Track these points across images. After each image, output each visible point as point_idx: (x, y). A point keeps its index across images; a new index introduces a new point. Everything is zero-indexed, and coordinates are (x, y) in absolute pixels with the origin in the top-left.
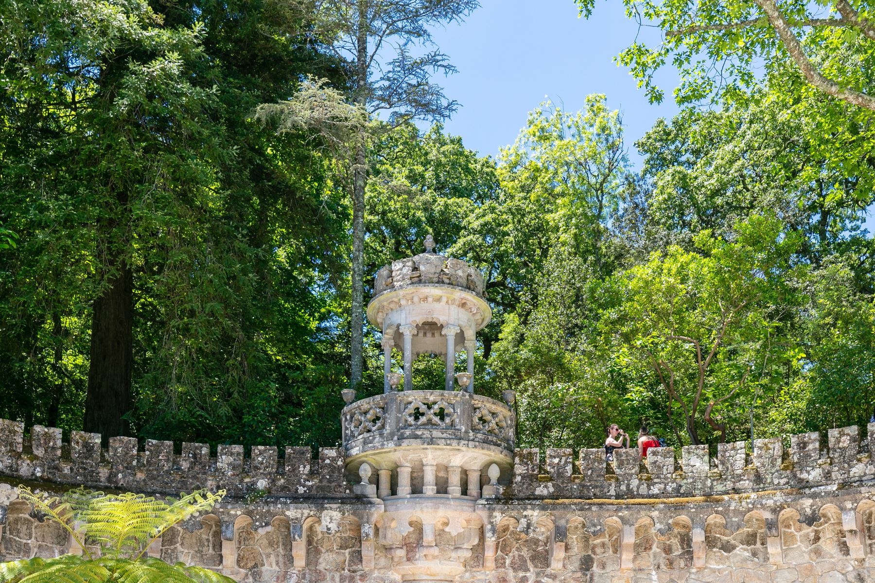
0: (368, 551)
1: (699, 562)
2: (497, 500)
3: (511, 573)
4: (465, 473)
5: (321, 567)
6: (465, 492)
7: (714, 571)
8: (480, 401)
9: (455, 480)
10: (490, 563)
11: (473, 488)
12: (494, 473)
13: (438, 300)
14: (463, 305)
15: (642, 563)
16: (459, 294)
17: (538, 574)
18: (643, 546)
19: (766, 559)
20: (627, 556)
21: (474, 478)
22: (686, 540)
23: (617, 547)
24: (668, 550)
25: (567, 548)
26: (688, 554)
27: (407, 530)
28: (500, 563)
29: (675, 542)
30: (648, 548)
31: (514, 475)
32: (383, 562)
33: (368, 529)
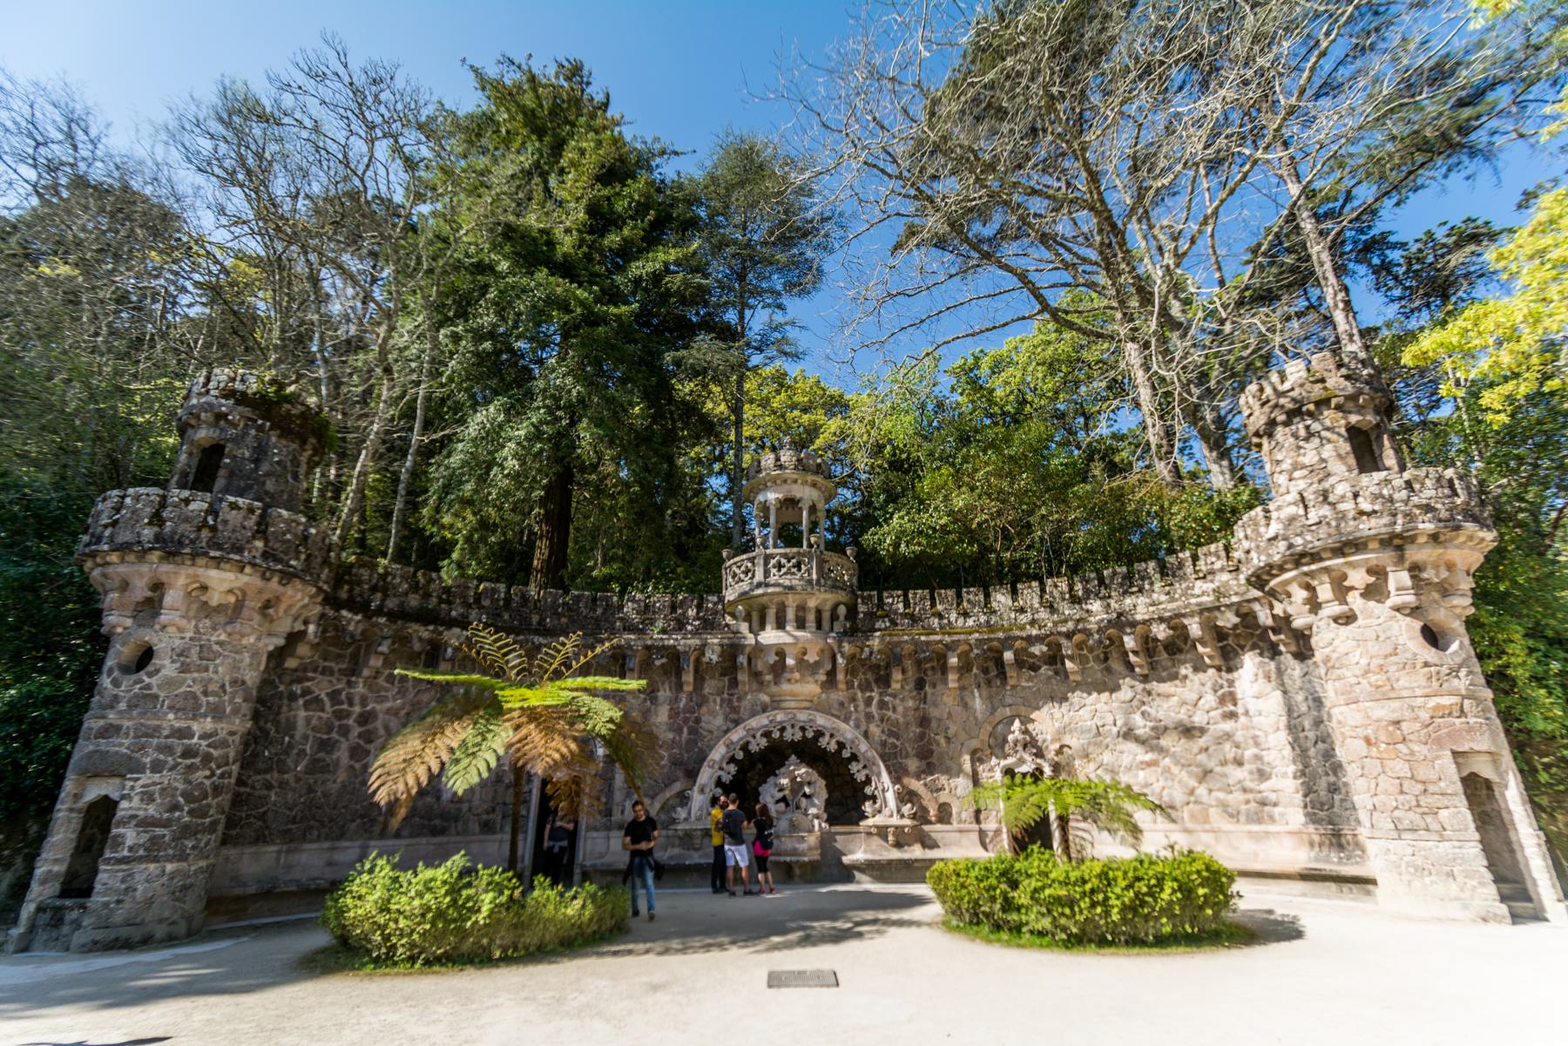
0: (743, 677)
1: (1012, 682)
2: (845, 633)
3: (859, 694)
4: (819, 612)
5: (706, 690)
6: (819, 626)
7: (1024, 688)
8: (828, 555)
9: (811, 617)
10: (842, 686)
11: (826, 624)
12: (842, 610)
13: (795, 481)
14: (814, 485)
15: (965, 682)
16: (810, 478)
17: (881, 694)
18: (965, 668)
19: (1067, 677)
20: (952, 677)
21: (826, 616)
22: (1000, 663)
23: (944, 669)
24: (985, 671)
25: (904, 672)
26: (1002, 675)
27: (772, 659)
28: (849, 685)
29: (991, 664)
30: (969, 670)
31: (857, 613)
32: (755, 686)
33: (742, 659)
